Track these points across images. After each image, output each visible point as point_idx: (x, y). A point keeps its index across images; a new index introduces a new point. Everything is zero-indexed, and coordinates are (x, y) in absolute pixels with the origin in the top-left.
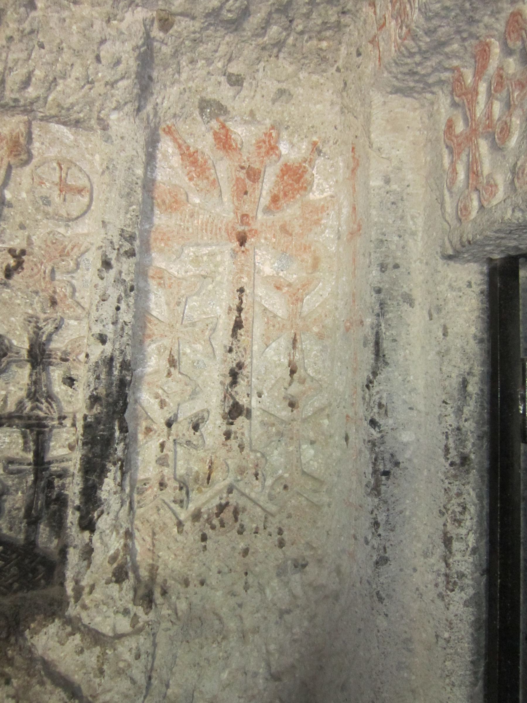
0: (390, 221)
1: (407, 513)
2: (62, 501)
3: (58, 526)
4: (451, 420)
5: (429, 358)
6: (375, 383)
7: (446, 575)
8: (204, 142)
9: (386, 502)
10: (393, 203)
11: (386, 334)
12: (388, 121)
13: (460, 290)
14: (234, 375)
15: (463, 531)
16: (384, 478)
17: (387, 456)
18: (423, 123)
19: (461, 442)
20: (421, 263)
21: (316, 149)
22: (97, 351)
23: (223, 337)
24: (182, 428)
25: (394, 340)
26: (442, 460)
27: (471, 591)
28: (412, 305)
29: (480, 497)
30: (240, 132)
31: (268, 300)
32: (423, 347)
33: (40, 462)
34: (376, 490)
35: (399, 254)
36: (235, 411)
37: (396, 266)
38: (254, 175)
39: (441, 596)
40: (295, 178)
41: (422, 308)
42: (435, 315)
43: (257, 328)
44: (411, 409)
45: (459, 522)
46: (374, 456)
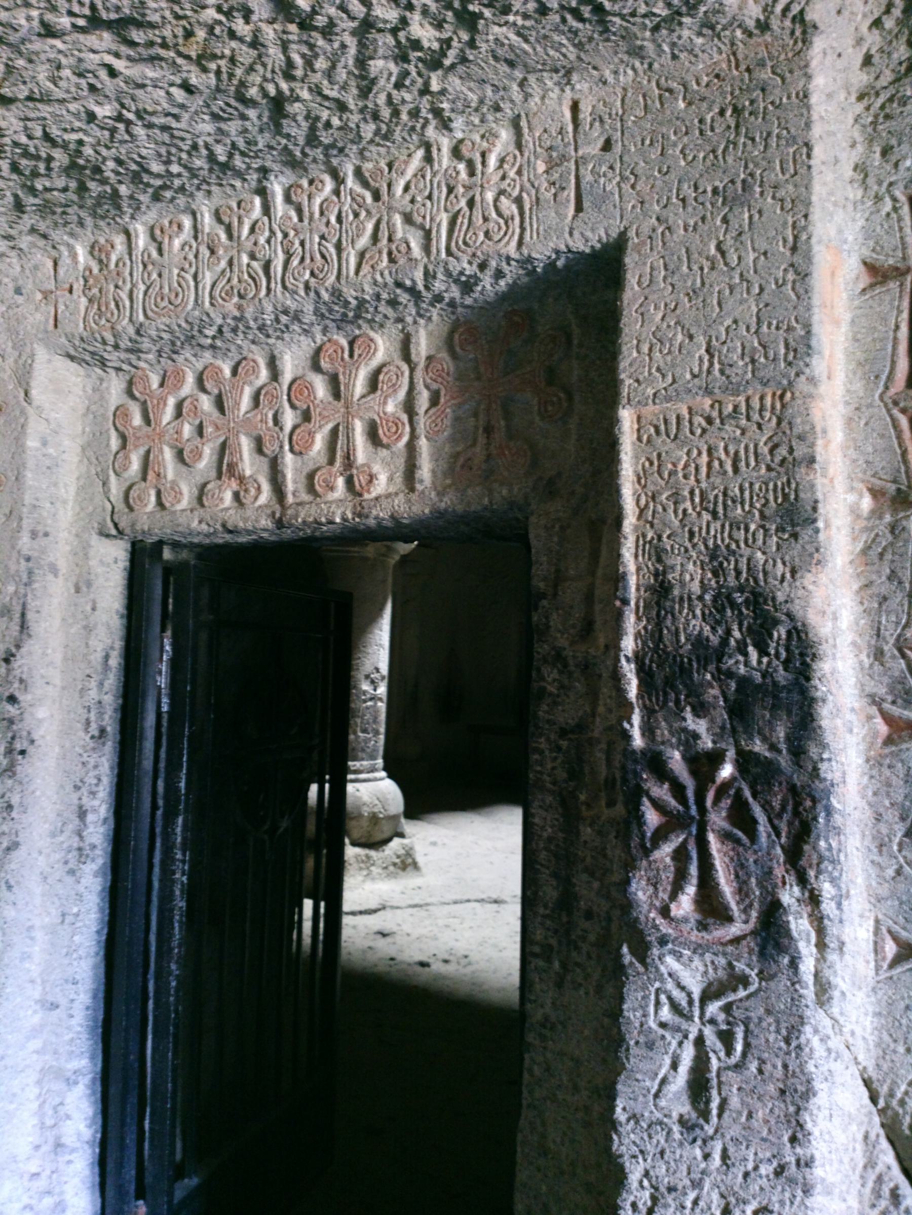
0: (44, 486)
1: (38, 793)
4: (93, 694)
5: (73, 631)
6: (18, 657)
7: (80, 849)
9: (21, 783)
10: (49, 468)
11: (32, 604)
12: (50, 380)
13: (108, 565)
15: (96, 803)
16: (20, 757)
17: (25, 734)
18: (84, 391)
19: (101, 714)
20: (69, 533)
25: (38, 612)
26: (81, 734)
27: (100, 861)
28: (56, 576)
29: (112, 768)
32: (63, 619)
35: (49, 522)
37: (46, 535)
39: (72, 872)
41: (66, 580)
42: (84, 589)
44: (48, 683)
45: (93, 794)
46: (10, 735)
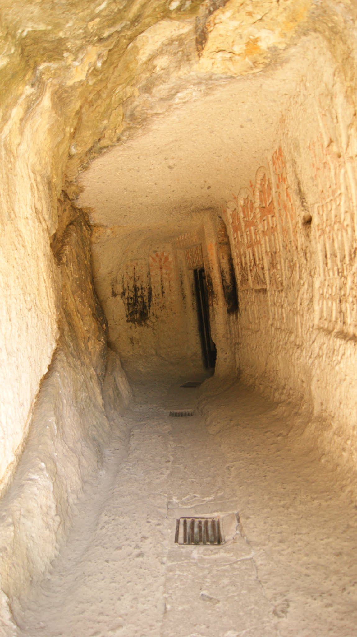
2: (146, 306)
3: (146, 309)
8: (154, 256)
14: (162, 288)
21: (169, 254)
22: (148, 287)
23: (160, 282)
24: (157, 296)
30: (159, 253)
31: (165, 276)
33: (143, 302)
34: (183, 299)
36: (163, 293)
38: (161, 259)
40: (167, 258)
43: (164, 280)
